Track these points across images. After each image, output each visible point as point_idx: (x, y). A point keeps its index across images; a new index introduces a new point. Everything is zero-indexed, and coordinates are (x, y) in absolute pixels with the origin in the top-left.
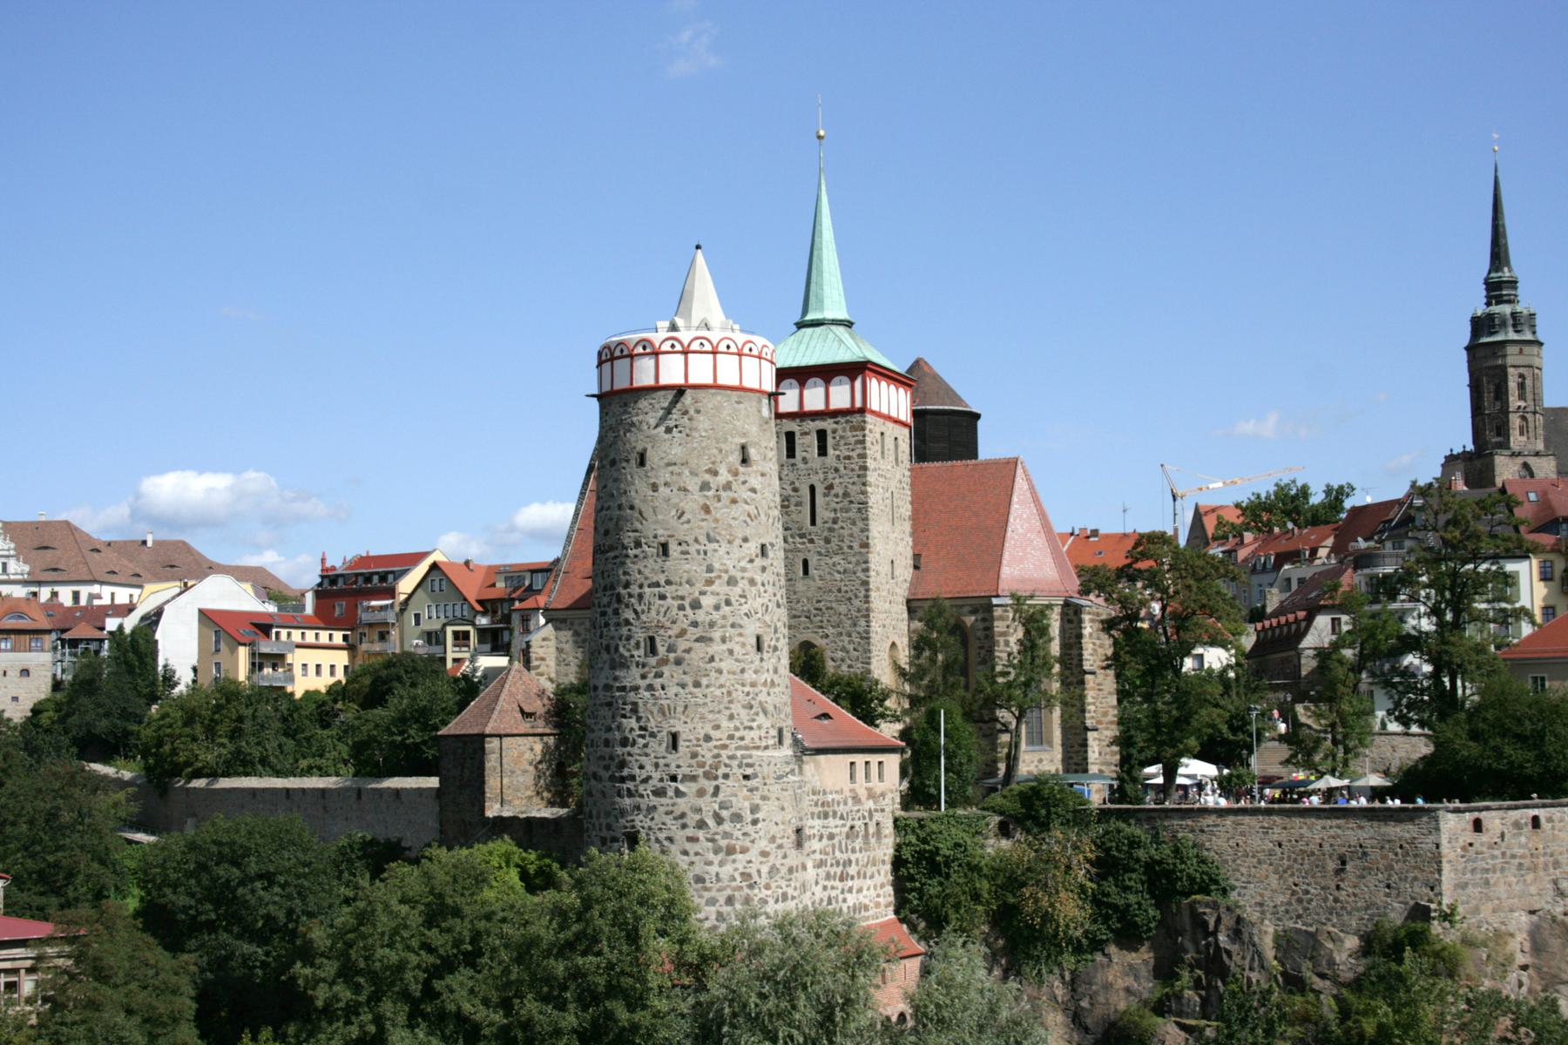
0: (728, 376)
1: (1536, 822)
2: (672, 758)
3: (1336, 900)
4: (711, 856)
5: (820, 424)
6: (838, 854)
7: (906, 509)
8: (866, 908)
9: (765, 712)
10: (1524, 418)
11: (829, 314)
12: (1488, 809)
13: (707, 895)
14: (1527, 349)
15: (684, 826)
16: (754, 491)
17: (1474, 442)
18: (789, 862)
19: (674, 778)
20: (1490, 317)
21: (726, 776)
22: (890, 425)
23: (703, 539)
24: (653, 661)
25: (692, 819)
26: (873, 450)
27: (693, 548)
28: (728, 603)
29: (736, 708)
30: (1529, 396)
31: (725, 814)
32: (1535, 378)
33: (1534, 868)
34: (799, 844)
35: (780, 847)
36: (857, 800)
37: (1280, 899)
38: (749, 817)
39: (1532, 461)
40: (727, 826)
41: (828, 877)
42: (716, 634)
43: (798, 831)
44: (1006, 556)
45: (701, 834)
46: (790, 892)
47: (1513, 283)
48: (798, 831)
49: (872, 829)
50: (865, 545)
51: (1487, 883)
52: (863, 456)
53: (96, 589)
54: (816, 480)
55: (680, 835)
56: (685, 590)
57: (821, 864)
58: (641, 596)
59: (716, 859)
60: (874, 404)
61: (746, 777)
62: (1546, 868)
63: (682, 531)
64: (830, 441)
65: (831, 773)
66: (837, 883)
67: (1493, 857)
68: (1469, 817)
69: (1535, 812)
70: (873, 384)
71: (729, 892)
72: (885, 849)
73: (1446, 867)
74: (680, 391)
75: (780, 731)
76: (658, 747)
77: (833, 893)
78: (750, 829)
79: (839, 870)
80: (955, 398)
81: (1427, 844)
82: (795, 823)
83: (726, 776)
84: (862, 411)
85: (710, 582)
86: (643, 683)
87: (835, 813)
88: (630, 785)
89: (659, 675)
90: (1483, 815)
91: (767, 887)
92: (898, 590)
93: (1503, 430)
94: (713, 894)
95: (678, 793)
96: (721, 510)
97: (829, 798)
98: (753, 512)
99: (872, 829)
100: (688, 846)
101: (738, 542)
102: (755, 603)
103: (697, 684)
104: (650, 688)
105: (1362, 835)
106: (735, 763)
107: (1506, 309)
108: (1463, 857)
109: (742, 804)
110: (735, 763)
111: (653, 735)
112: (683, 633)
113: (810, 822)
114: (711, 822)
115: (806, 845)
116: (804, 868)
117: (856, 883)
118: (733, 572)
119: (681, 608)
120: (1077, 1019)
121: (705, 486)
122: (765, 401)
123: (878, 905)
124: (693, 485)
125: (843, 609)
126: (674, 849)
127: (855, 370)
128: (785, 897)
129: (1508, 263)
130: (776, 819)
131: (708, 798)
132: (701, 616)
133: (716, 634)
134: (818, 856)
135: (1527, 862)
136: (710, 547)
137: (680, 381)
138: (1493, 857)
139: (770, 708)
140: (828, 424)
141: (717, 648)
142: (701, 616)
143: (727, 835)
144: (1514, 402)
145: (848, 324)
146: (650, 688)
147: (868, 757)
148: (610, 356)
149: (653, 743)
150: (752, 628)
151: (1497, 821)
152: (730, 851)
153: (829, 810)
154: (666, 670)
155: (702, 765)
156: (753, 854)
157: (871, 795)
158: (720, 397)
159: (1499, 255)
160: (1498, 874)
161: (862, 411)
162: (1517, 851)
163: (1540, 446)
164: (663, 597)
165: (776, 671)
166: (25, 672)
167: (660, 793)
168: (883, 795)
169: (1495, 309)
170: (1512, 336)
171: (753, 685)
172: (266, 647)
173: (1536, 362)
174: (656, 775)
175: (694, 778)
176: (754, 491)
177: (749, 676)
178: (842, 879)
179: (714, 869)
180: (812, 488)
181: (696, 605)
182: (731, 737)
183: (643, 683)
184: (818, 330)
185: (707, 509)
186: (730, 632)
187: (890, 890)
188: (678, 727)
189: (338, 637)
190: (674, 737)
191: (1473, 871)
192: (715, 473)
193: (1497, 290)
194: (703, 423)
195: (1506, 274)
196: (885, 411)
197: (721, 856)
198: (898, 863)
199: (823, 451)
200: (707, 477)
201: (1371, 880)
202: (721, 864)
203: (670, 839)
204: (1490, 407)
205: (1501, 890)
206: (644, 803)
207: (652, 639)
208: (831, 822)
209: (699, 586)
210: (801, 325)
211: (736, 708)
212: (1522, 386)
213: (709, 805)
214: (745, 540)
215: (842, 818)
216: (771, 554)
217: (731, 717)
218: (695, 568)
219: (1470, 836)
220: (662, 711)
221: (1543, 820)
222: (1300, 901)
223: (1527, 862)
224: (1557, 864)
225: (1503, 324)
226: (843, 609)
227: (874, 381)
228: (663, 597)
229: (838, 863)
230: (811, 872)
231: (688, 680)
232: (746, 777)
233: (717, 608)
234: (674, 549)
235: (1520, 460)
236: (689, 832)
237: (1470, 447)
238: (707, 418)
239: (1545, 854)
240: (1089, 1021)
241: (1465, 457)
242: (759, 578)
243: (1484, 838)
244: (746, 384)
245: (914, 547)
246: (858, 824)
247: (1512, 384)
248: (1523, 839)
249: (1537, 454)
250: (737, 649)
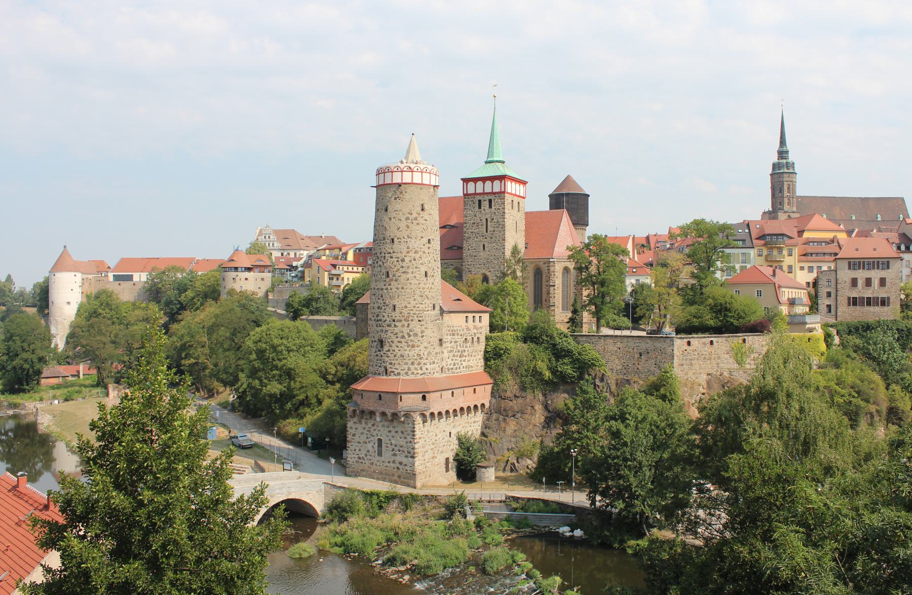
0: (417, 178)
1: (712, 342)
2: (393, 314)
3: (638, 369)
4: (406, 348)
5: (490, 197)
6: (459, 348)
7: (523, 228)
8: (472, 367)
9: (428, 298)
10: (789, 199)
11: (495, 159)
12: (693, 337)
13: (405, 361)
14: (791, 175)
15: (397, 337)
16: (426, 220)
17: (772, 207)
18: (435, 351)
19: (394, 321)
20: (779, 163)
21: (412, 320)
22: (517, 198)
23: (406, 237)
24: (388, 280)
25: (400, 335)
26: (508, 207)
27: (402, 240)
28: (415, 260)
29: (416, 297)
30: (791, 192)
31: (411, 333)
32: (794, 186)
33: (710, 359)
34: (441, 345)
35: (432, 345)
36: (468, 329)
37: (619, 367)
38: (420, 335)
39: (790, 214)
40: (412, 338)
41: (454, 356)
42: (410, 271)
43: (440, 340)
44: (557, 244)
45: (403, 340)
46: (436, 361)
47: (787, 152)
48: (440, 340)
49: (475, 339)
50: (504, 240)
51: (691, 364)
52: (504, 208)
53: (302, 252)
54: (488, 216)
55: (396, 340)
56: (399, 255)
57: (451, 351)
58: (385, 257)
59: (408, 349)
60: (509, 190)
61: (419, 321)
62: (715, 359)
63: (399, 234)
64: (493, 203)
65: (457, 320)
66: (458, 358)
67: (694, 355)
68: (686, 340)
69: (712, 339)
70: (509, 183)
71: (412, 360)
72: (482, 347)
73: (675, 357)
74: (400, 185)
75: (434, 305)
76: (389, 310)
77: (456, 362)
78: (420, 339)
79: (459, 354)
80: (580, 188)
81: (669, 350)
82: (439, 337)
83: (412, 320)
84: (504, 192)
85: (408, 252)
86: (385, 287)
87: (458, 334)
88: (380, 322)
89: (390, 285)
90: (691, 340)
91: (427, 359)
93: (781, 203)
94: (406, 361)
95: (395, 326)
96: (414, 227)
97: (456, 328)
98: (425, 228)
99: (475, 339)
100: (398, 344)
101: (419, 238)
102: (425, 260)
103: (403, 288)
104: (387, 289)
105: (648, 346)
106: (415, 316)
107: (784, 161)
109: (418, 330)
110: (415, 316)
111: (387, 306)
112: (398, 270)
113: (446, 337)
114: (406, 336)
115: (444, 345)
116: (443, 353)
117: (467, 358)
118: (417, 249)
119: (398, 261)
120: (546, 407)
121: (407, 219)
122: (432, 189)
123: (477, 366)
124: (403, 219)
125: (496, 262)
126: (393, 345)
127: (502, 178)
128: (434, 363)
129: (785, 145)
130: (431, 334)
131: (405, 328)
132: (404, 264)
133: (410, 271)
134: (449, 349)
135: (707, 357)
136: (409, 240)
137: (400, 182)
138: (694, 355)
139: (430, 297)
140: (492, 197)
141: (410, 276)
142: (404, 264)
143: (412, 341)
144: (786, 194)
145: (503, 162)
146: (387, 289)
147: (474, 315)
148: (380, 172)
149: (387, 308)
150: (423, 269)
152: (413, 346)
153: (456, 333)
154: (392, 283)
155: (404, 316)
156: (422, 347)
157: (475, 327)
158: (413, 187)
159: (783, 142)
161: (504, 192)
163: (795, 209)
164: (392, 257)
165: (433, 284)
166: (263, 279)
167: (389, 326)
168: (481, 328)
169: (781, 161)
170: (786, 171)
171: (423, 289)
172: (334, 272)
173: (794, 180)
174: (388, 319)
175: (400, 321)
176: (426, 220)
177: (422, 285)
178: (460, 357)
179: (407, 352)
180: (487, 219)
181: (403, 260)
182: (414, 307)
183: (385, 287)
184: (492, 164)
185: (408, 227)
186: (415, 270)
187: (482, 360)
188: (396, 303)
189: (360, 269)
190: (394, 306)
191: (686, 360)
192: (411, 214)
193: (782, 154)
194: (407, 196)
195: (785, 149)
196: (513, 192)
197: (410, 348)
198: (486, 352)
199: (490, 206)
200: (408, 215)
201: (649, 362)
202: (410, 351)
203: (392, 342)
204: (778, 195)
205: (697, 367)
206: (384, 329)
207: (388, 272)
208: (456, 337)
209: (404, 254)
210: (486, 162)
211: (416, 297)
212: (789, 188)
213: (406, 330)
214: (422, 237)
215: (461, 335)
216: (432, 242)
217: (415, 300)
218: (403, 247)
219: (686, 347)
220: (390, 297)
221: (714, 342)
222: (625, 368)
223: (707, 357)
224: (719, 358)
225: (783, 167)
226: (496, 262)
227: (509, 182)
228: (392, 257)
229: (459, 351)
230: (446, 354)
231: (400, 286)
232: (419, 321)
233: (410, 261)
234: (396, 240)
235: (787, 214)
236: (399, 339)
237: (771, 209)
238: (410, 194)
240: (550, 408)
241: (769, 212)
242: (427, 251)
243: (691, 348)
244: (424, 182)
245: (526, 241)
246: (469, 338)
247: (785, 188)
248: (706, 349)
249: (793, 212)
250: (417, 276)
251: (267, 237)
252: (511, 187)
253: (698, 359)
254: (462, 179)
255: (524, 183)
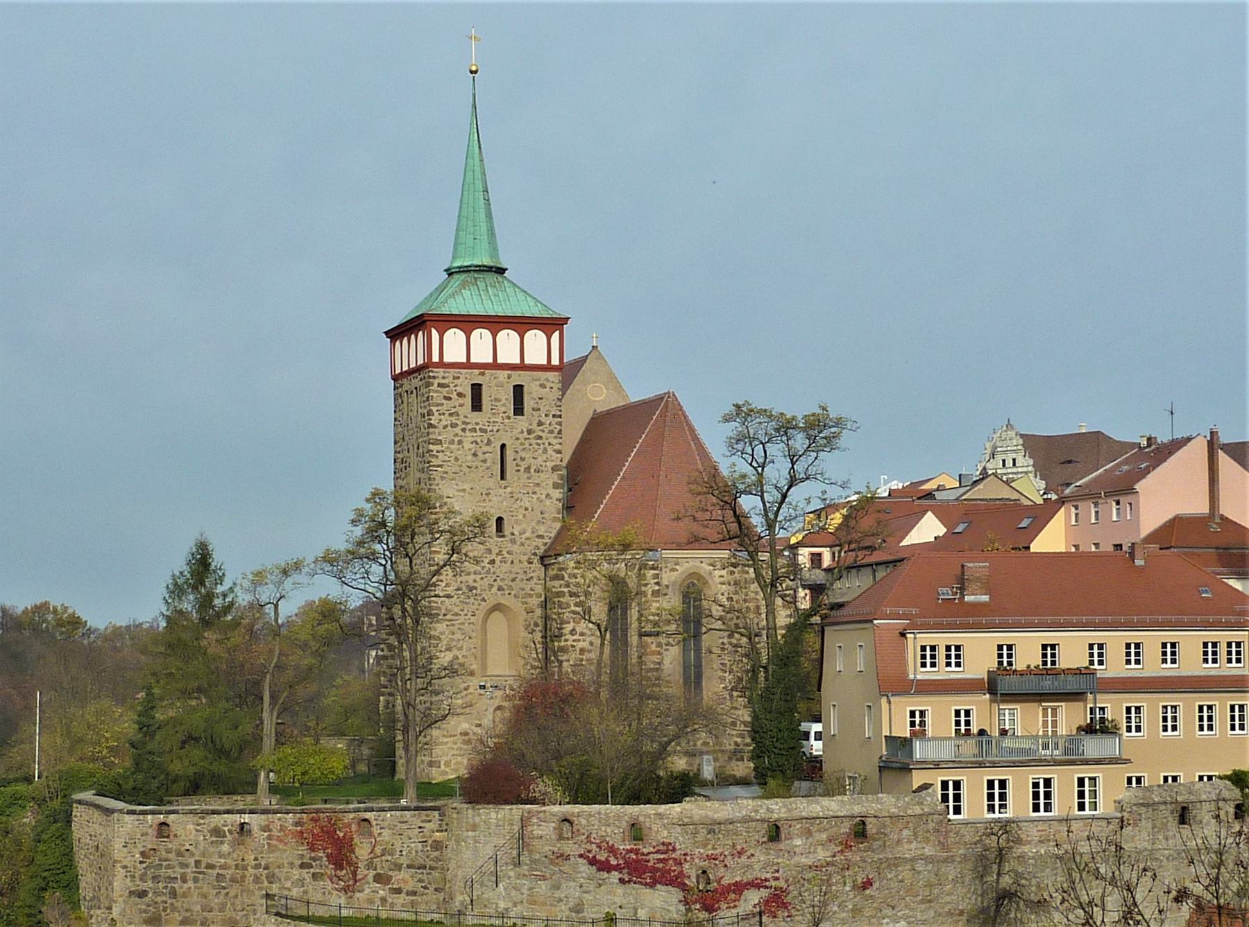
51: (173, 894)
69: (246, 818)
92: (515, 548)
108: (141, 862)
151: (191, 827)
160: (190, 884)
162: (215, 860)
191: (155, 878)
224: (271, 879)
239: (257, 866)
248: (225, 848)
251: (1009, 463)
252: (453, 345)
253: (196, 880)
254: (386, 333)
255: (551, 325)
